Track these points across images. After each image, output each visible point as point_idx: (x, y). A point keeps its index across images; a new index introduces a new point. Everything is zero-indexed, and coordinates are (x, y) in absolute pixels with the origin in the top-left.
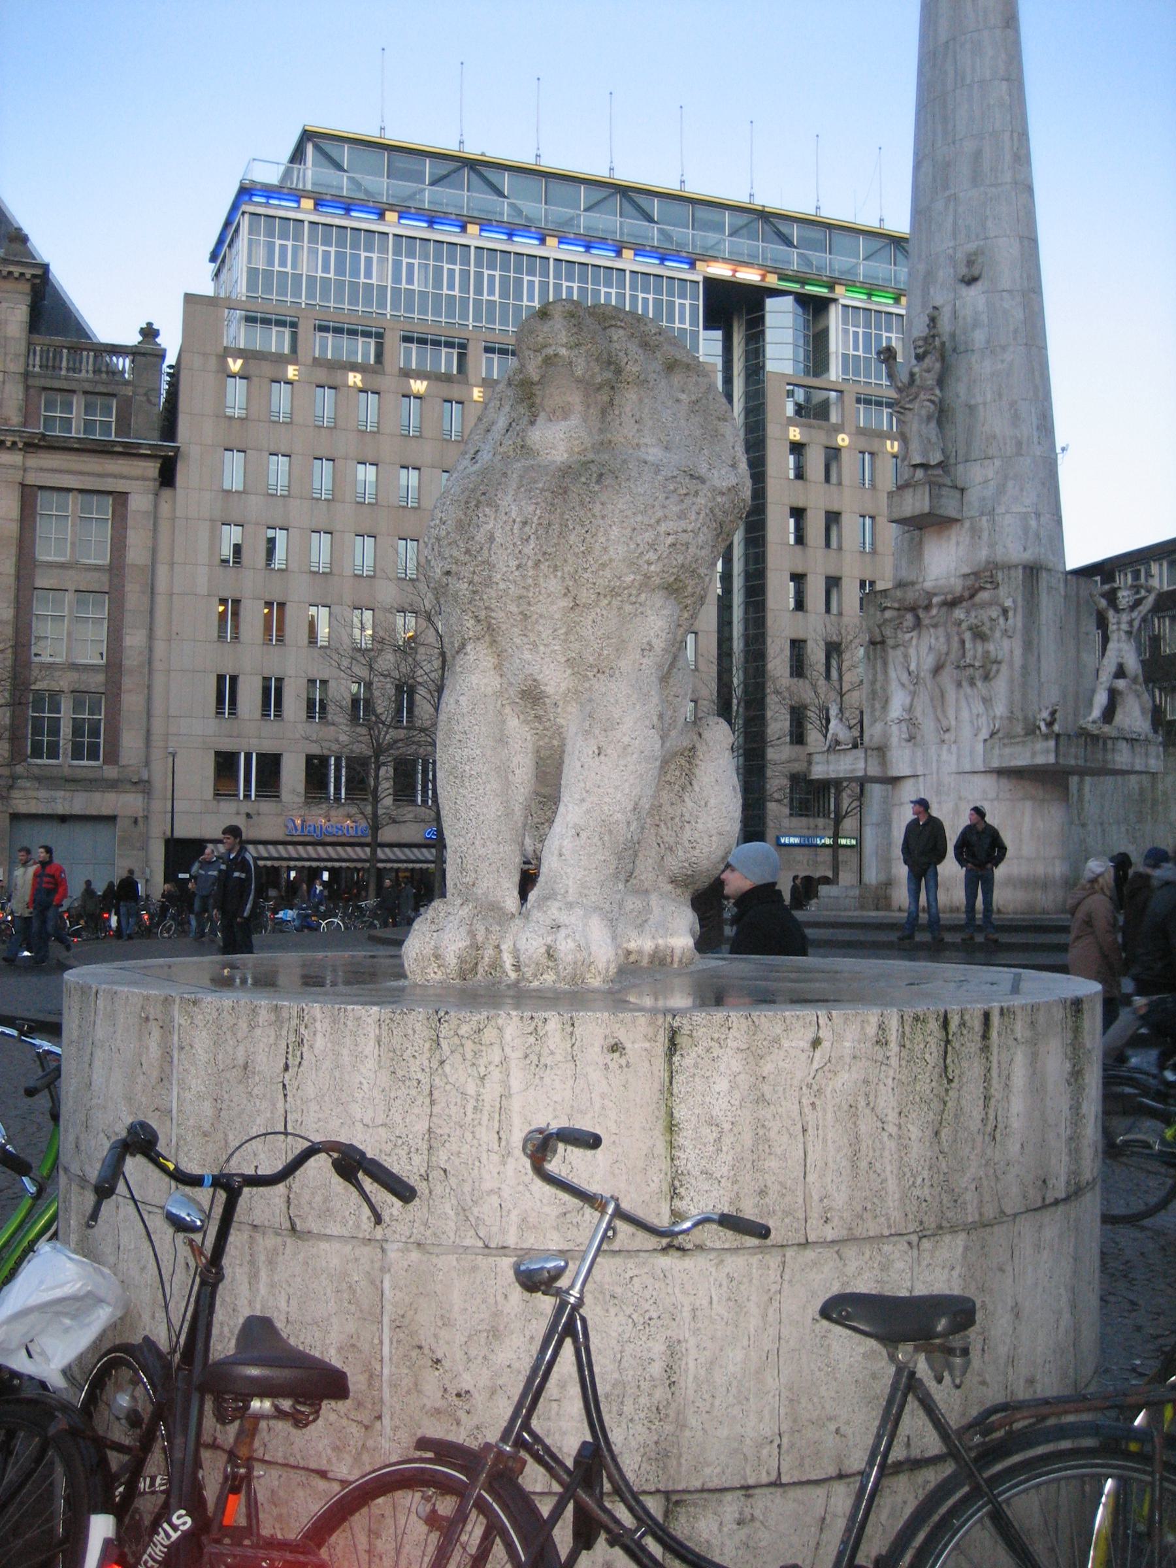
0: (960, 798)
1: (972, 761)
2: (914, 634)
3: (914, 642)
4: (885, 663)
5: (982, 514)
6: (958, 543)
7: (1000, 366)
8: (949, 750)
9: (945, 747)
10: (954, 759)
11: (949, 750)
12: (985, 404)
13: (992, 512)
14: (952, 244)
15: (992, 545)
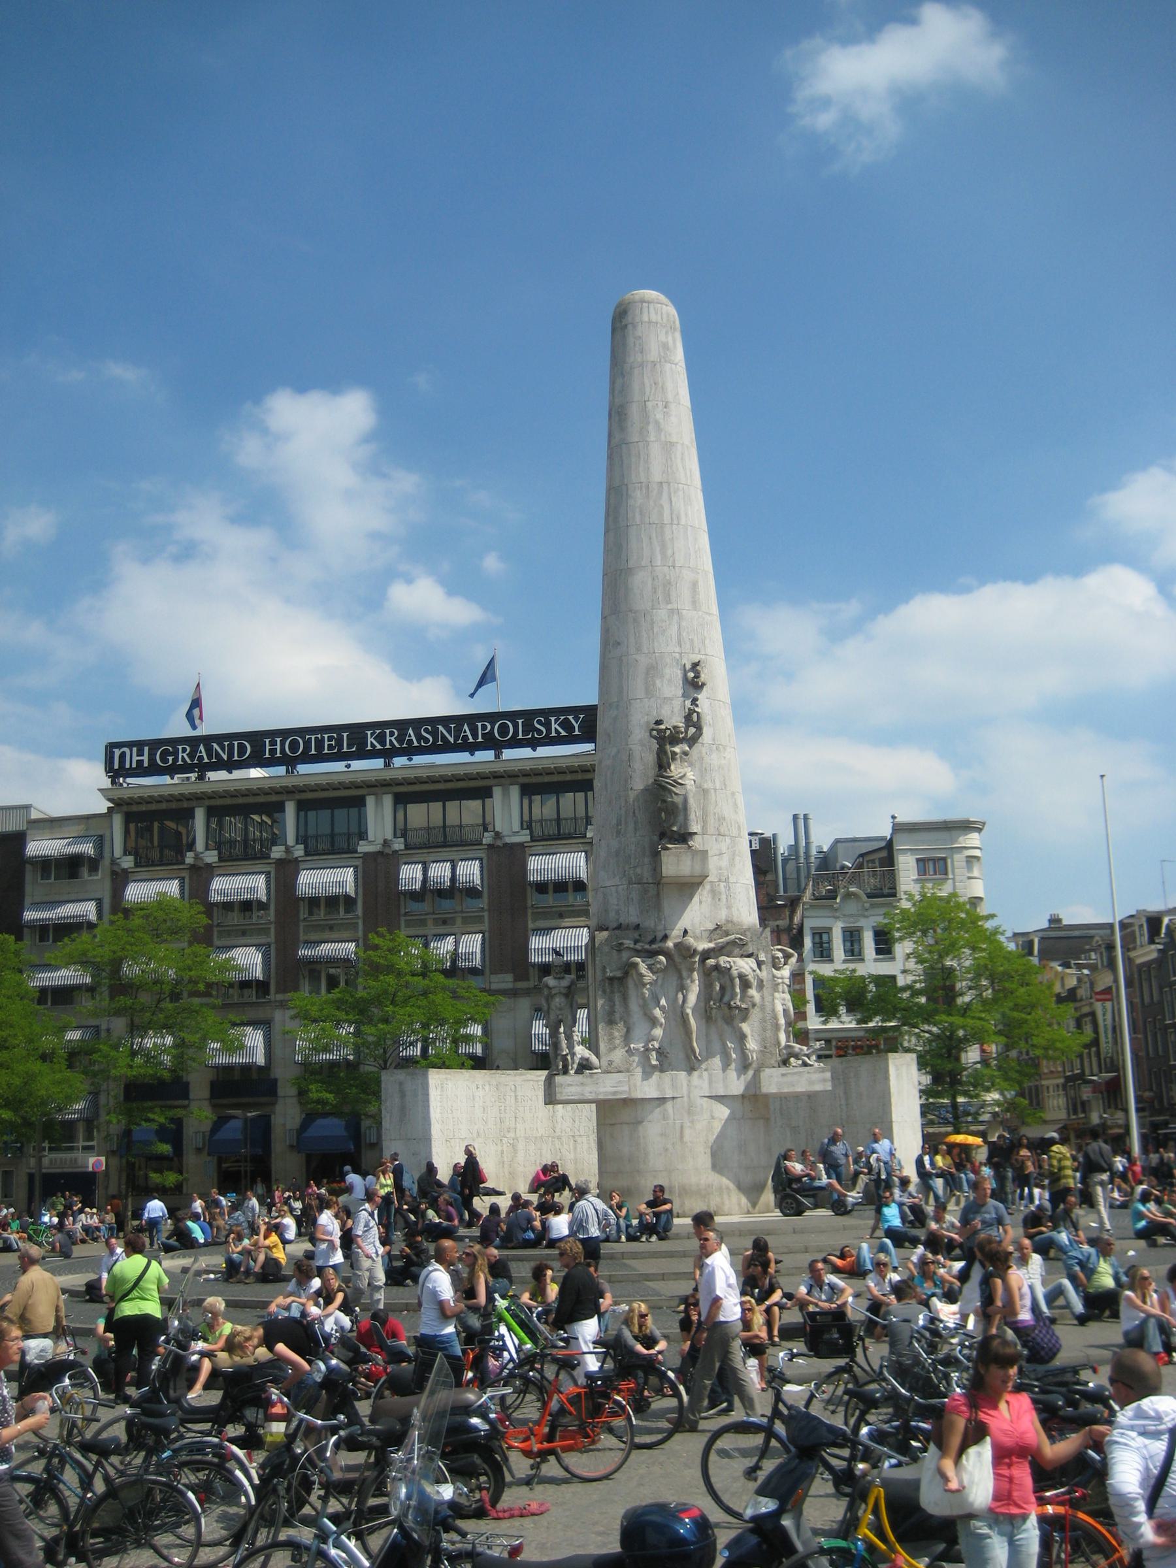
0: (713, 1118)
1: (726, 1087)
2: (661, 975)
3: (660, 982)
4: (625, 998)
5: (720, 880)
6: (701, 902)
7: (723, 762)
8: (700, 1076)
9: (696, 1074)
10: (705, 1085)
11: (700, 1076)
12: (715, 790)
13: (727, 880)
14: (677, 650)
15: (729, 907)
